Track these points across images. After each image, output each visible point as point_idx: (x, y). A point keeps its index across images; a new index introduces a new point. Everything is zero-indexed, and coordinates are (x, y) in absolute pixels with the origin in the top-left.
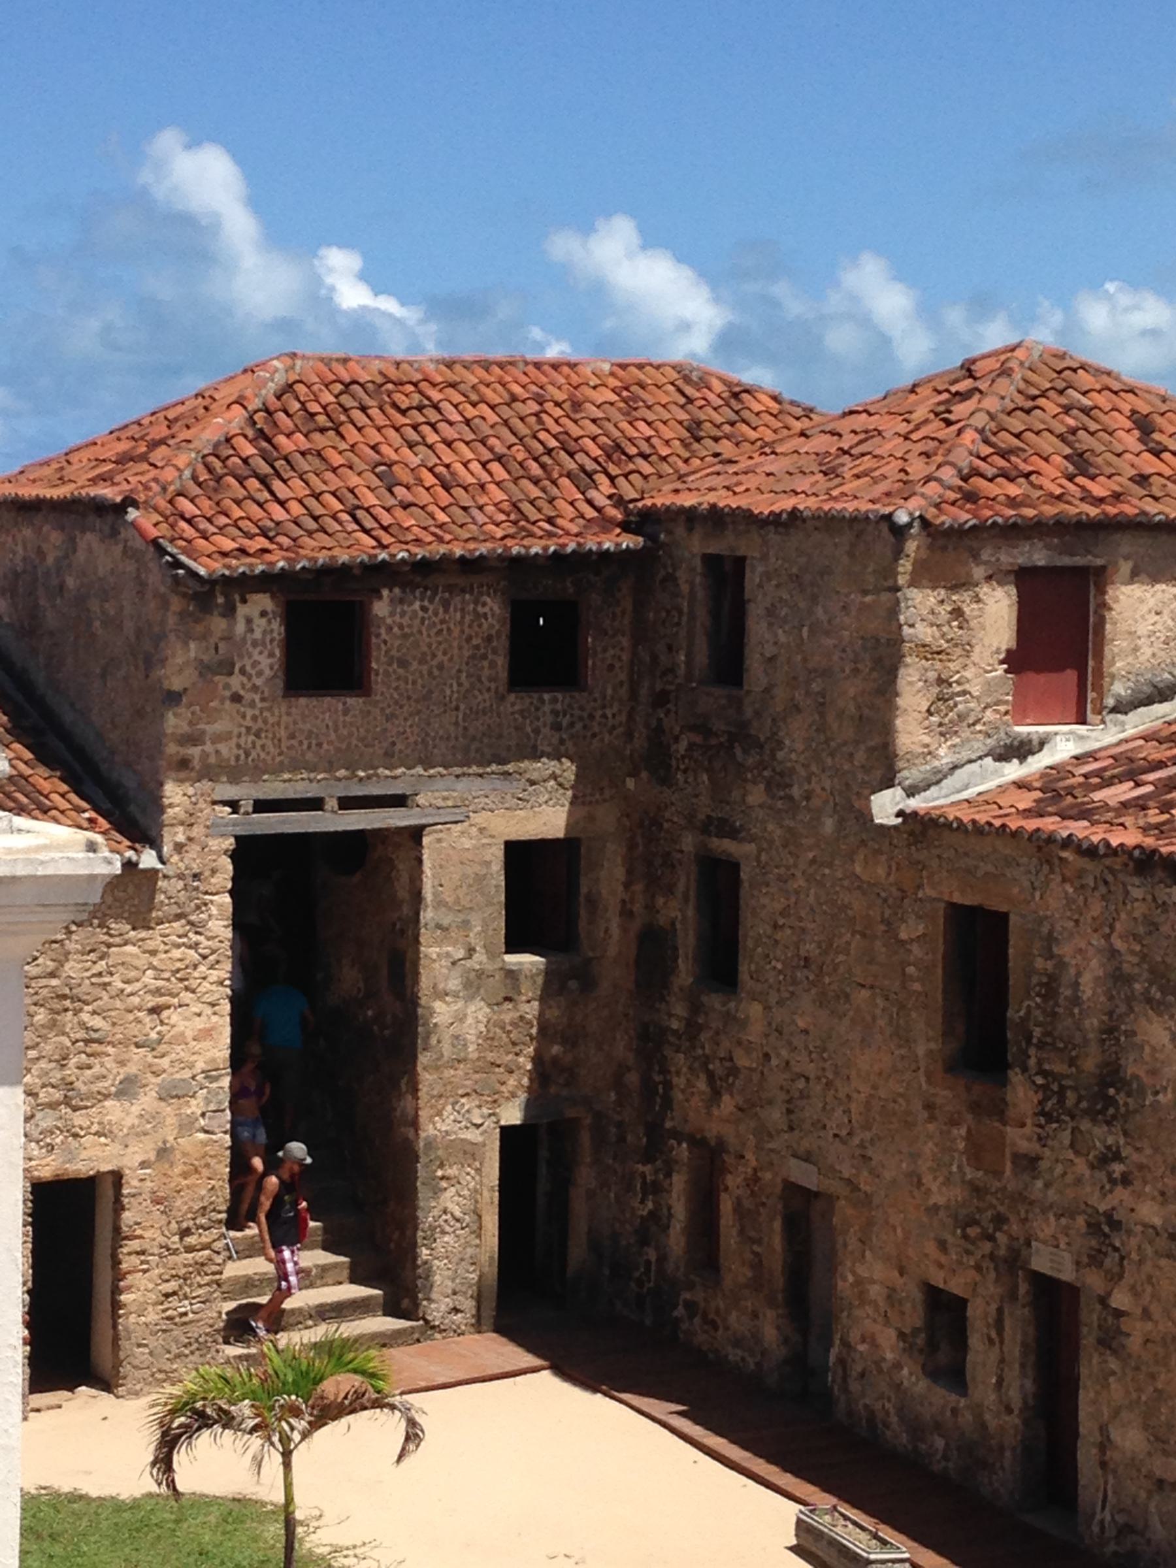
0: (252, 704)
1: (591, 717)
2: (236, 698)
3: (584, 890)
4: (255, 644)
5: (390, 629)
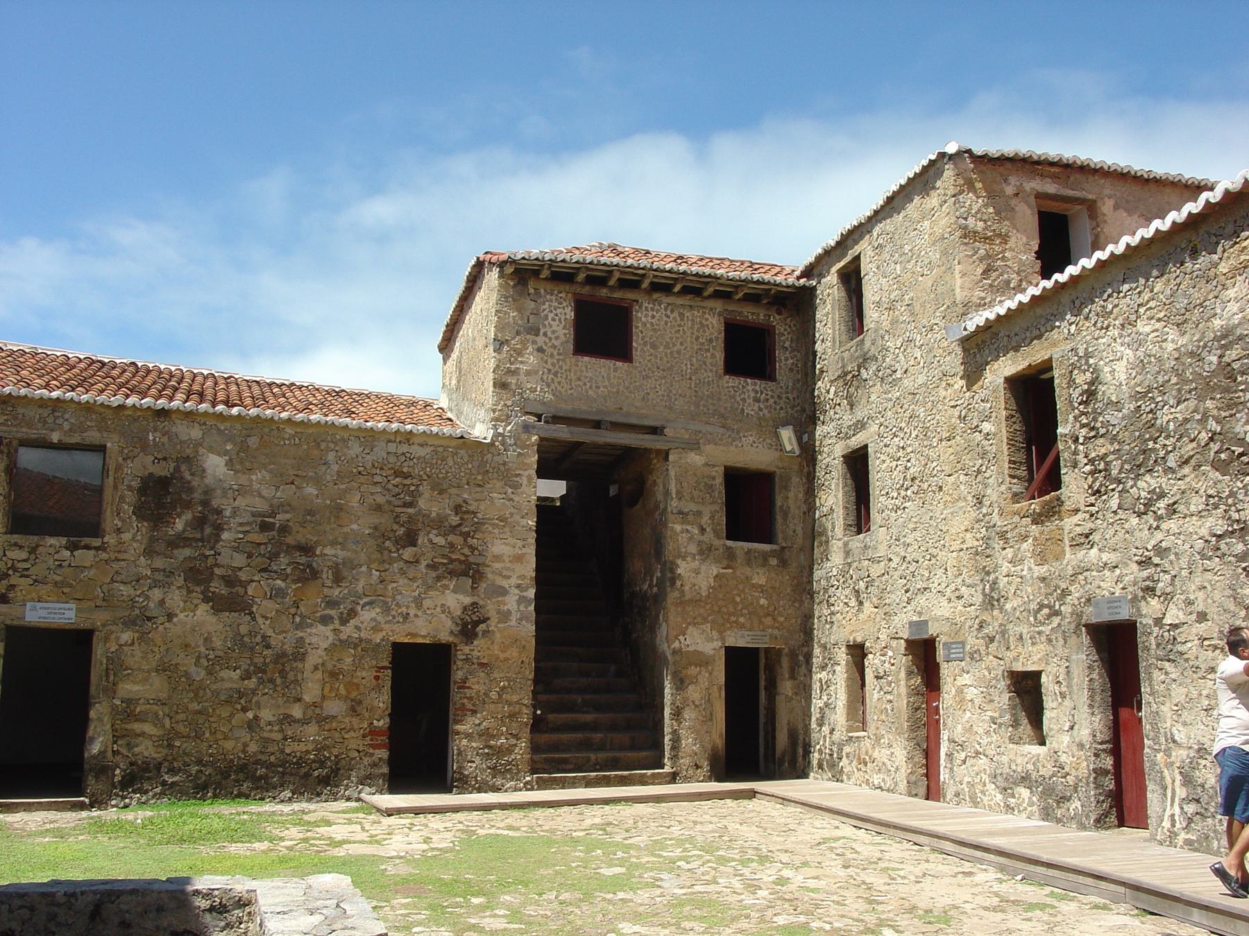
0: (552, 356)
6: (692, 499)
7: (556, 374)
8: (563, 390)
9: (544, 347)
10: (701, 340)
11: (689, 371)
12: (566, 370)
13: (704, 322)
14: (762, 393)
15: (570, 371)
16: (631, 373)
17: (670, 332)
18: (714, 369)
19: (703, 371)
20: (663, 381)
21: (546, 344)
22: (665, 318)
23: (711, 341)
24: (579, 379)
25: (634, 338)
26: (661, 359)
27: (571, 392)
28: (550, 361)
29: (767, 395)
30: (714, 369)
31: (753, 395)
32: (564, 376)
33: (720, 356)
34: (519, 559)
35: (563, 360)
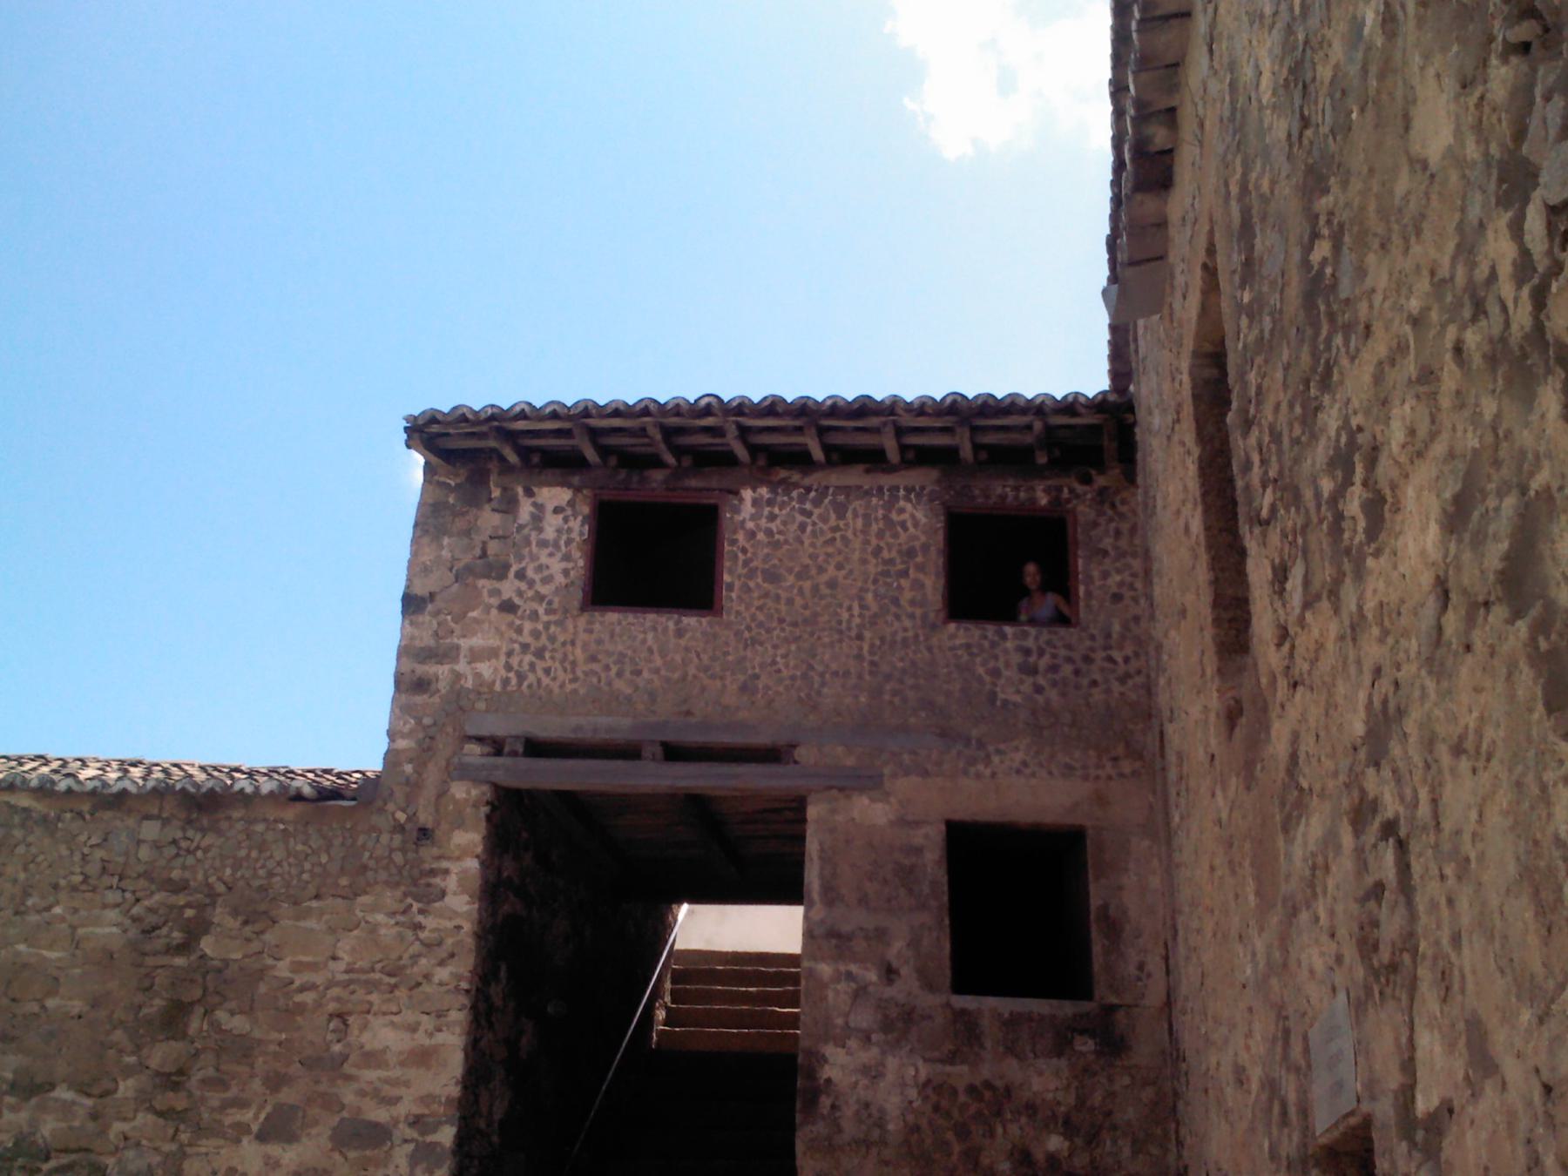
0: (534, 616)
1: (1087, 659)
2: (508, 607)
3: (1095, 902)
4: (543, 544)
5: (752, 535)
6: (863, 901)
7: (539, 654)
8: (555, 687)
9: (517, 601)
10: (886, 554)
11: (857, 620)
12: (564, 644)
13: (894, 516)
14: (1041, 653)
15: (573, 643)
16: (715, 636)
17: (813, 545)
18: (918, 612)
19: (890, 618)
20: (793, 647)
21: (520, 594)
22: (800, 518)
23: (910, 553)
24: (593, 659)
25: (727, 564)
26: (790, 602)
27: (574, 686)
28: (528, 626)
29: (1054, 656)
30: (918, 612)
32: (559, 656)
33: (933, 586)
34: (423, 1057)
35: (559, 623)
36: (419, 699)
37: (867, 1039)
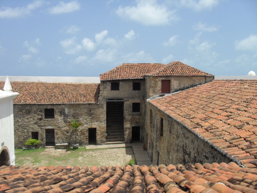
2: (106, 91)
6: (128, 108)
31: (137, 93)
33: (132, 88)
34: (104, 117)
36: (102, 97)
37: (128, 115)
